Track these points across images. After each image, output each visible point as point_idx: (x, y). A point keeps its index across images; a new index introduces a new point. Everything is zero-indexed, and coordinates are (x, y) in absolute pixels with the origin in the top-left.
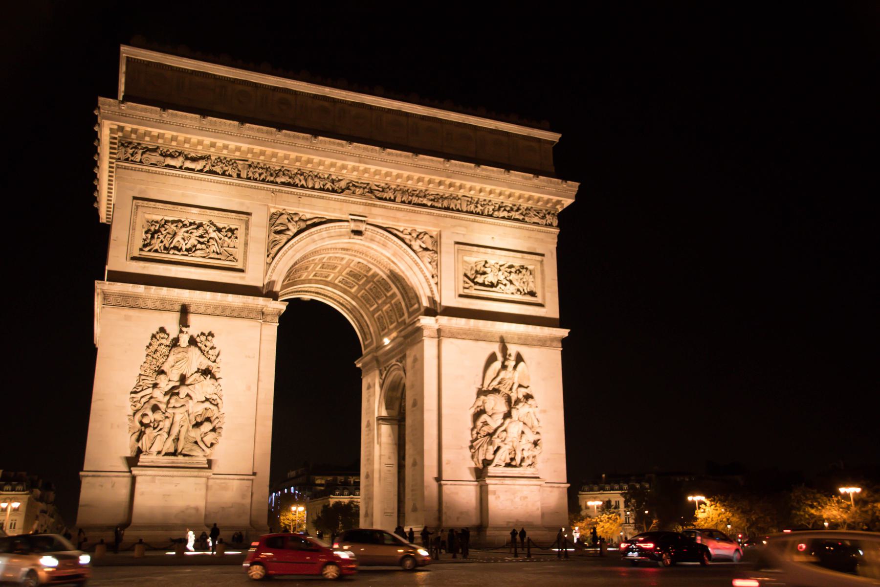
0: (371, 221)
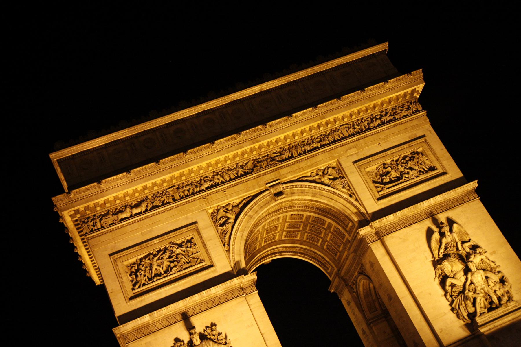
0: (284, 180)
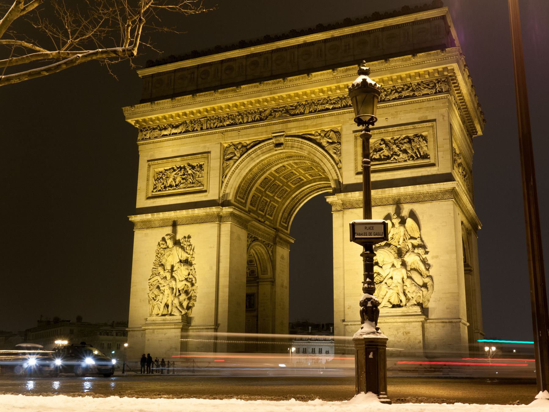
0: (289, 133)
